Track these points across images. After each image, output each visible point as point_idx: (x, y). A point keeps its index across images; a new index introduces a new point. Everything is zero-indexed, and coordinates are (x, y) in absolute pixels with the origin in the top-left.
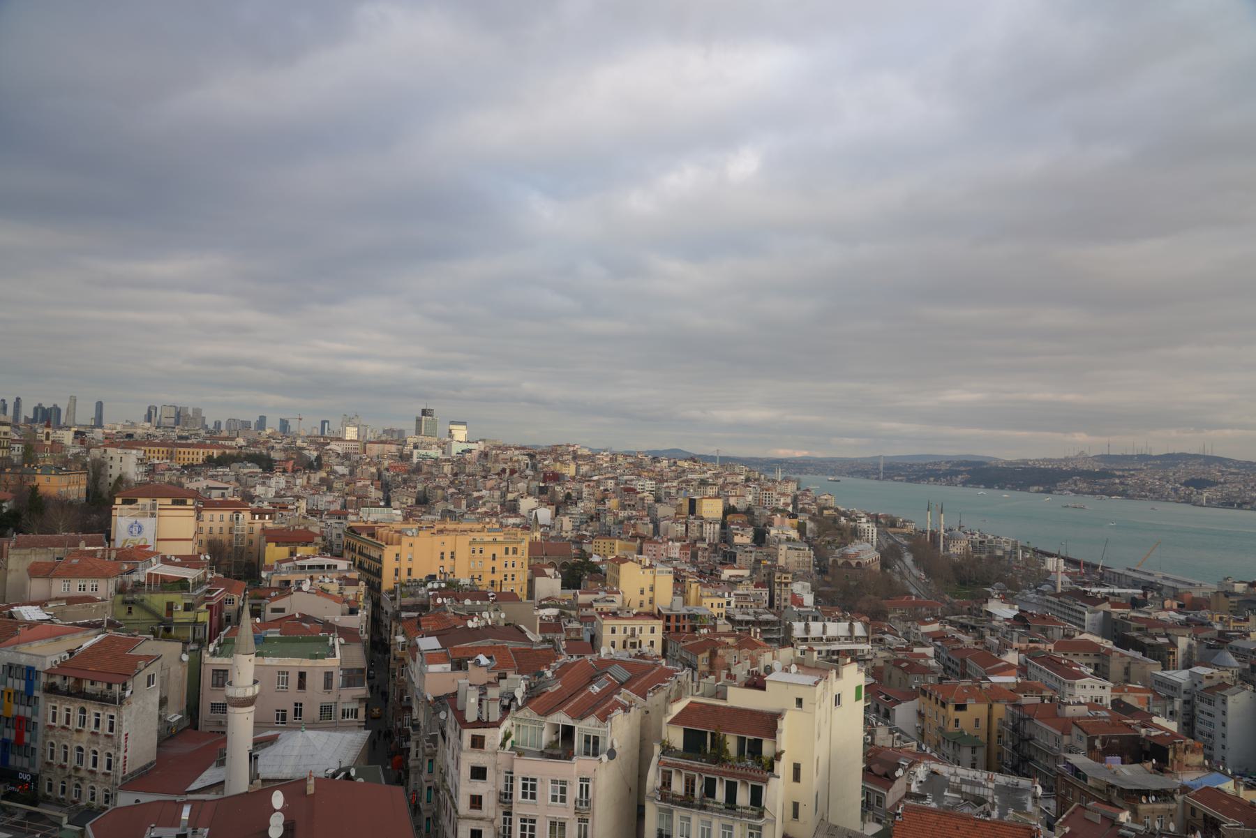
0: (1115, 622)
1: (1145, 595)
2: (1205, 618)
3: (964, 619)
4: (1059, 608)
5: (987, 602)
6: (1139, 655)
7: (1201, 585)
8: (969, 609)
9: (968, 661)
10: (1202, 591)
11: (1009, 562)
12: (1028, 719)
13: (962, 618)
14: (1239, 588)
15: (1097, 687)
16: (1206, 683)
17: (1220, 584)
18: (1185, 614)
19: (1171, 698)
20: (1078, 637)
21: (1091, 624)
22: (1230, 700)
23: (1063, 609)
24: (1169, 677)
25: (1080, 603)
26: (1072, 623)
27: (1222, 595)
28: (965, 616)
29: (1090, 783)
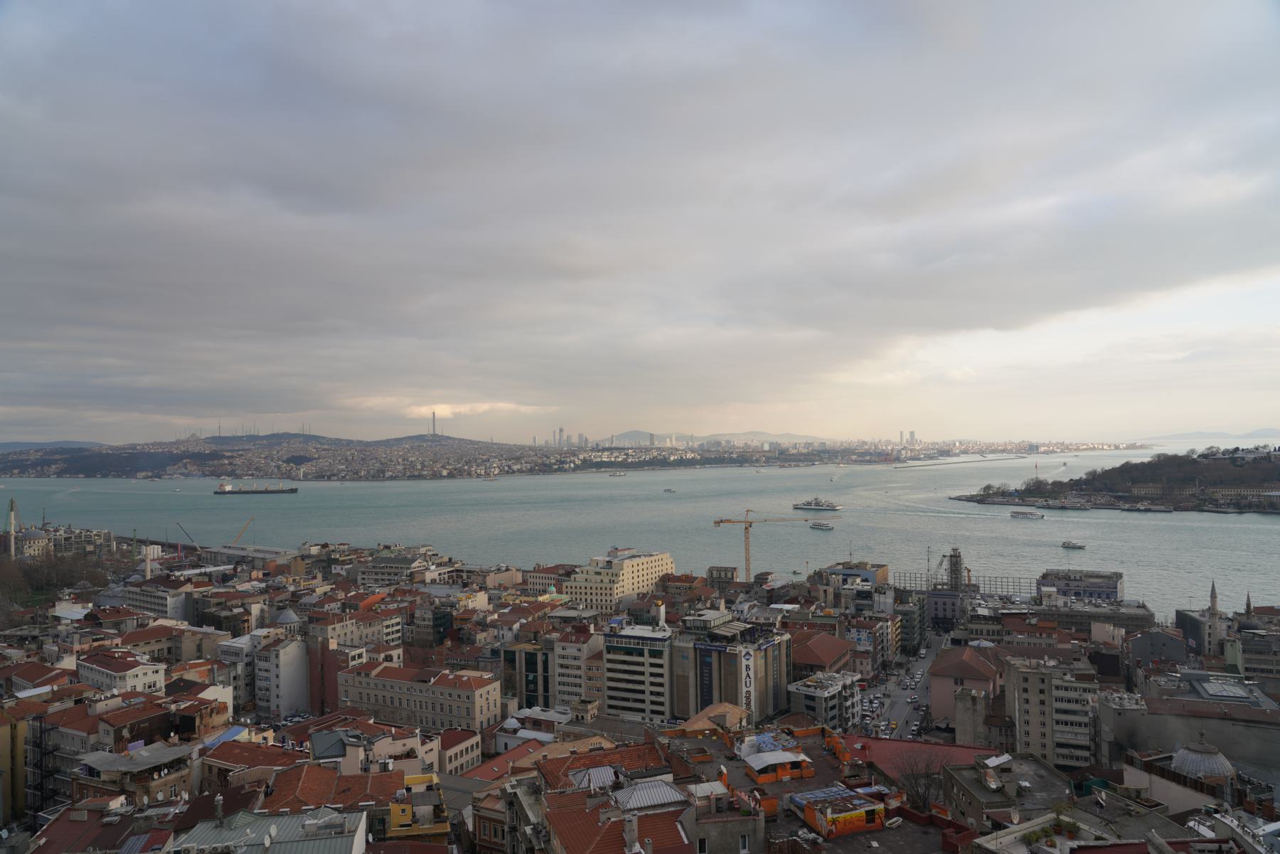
0: (196, 601)
1: (235, 569)
2: (281, 582)
3: (26, 631)
4: (142, 598)
5: (54, 606)
6: (211, 629)
7: (285, 552)
8: (32, 618)
9: (14, 678)
10: (287, 557)
11: (100, 557)
12: (52, 729)
13: (21, 630)
14: (315, 550)
15: (150, 673)
16: (264, 642)
17: (299, 549)
18: (267, 581)
19: (235, 664)
20: (152, 624)
21: (174, 608)
22: (282, 652)
23: (145, 599)
24: (233, 645)
25: (162, 588)
26: (147, 609)
27: (299, 559)
28: (25, 627)
29: (103, 777)
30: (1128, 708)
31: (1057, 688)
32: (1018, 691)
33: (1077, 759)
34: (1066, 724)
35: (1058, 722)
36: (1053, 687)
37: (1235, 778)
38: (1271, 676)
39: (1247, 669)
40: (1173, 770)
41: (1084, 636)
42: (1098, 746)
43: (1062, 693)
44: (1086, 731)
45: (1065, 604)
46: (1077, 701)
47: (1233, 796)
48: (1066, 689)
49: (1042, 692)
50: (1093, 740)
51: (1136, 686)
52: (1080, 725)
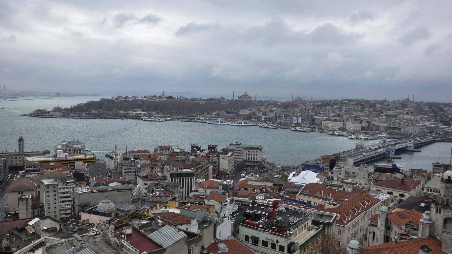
30: (85, 192)
31: (60, 189)
32: (45, 192)
33: (68, 214)
34: (64, 202)
35: (61, 202)
36: (59, 189)
37: (116, 209)
38: (131, 173)
39: (125, 172)
40: (97, 211)
41: (73, 167)
42: (74, 208)
43: (62, 191)
44: (70, 203)
45: (66, 156)
46: (68, 193)
47: (115, 215)
48: (64, 188)
49: (55, 191)
50: (73, 206)
51: (90, 184)
52: (69, 201)
